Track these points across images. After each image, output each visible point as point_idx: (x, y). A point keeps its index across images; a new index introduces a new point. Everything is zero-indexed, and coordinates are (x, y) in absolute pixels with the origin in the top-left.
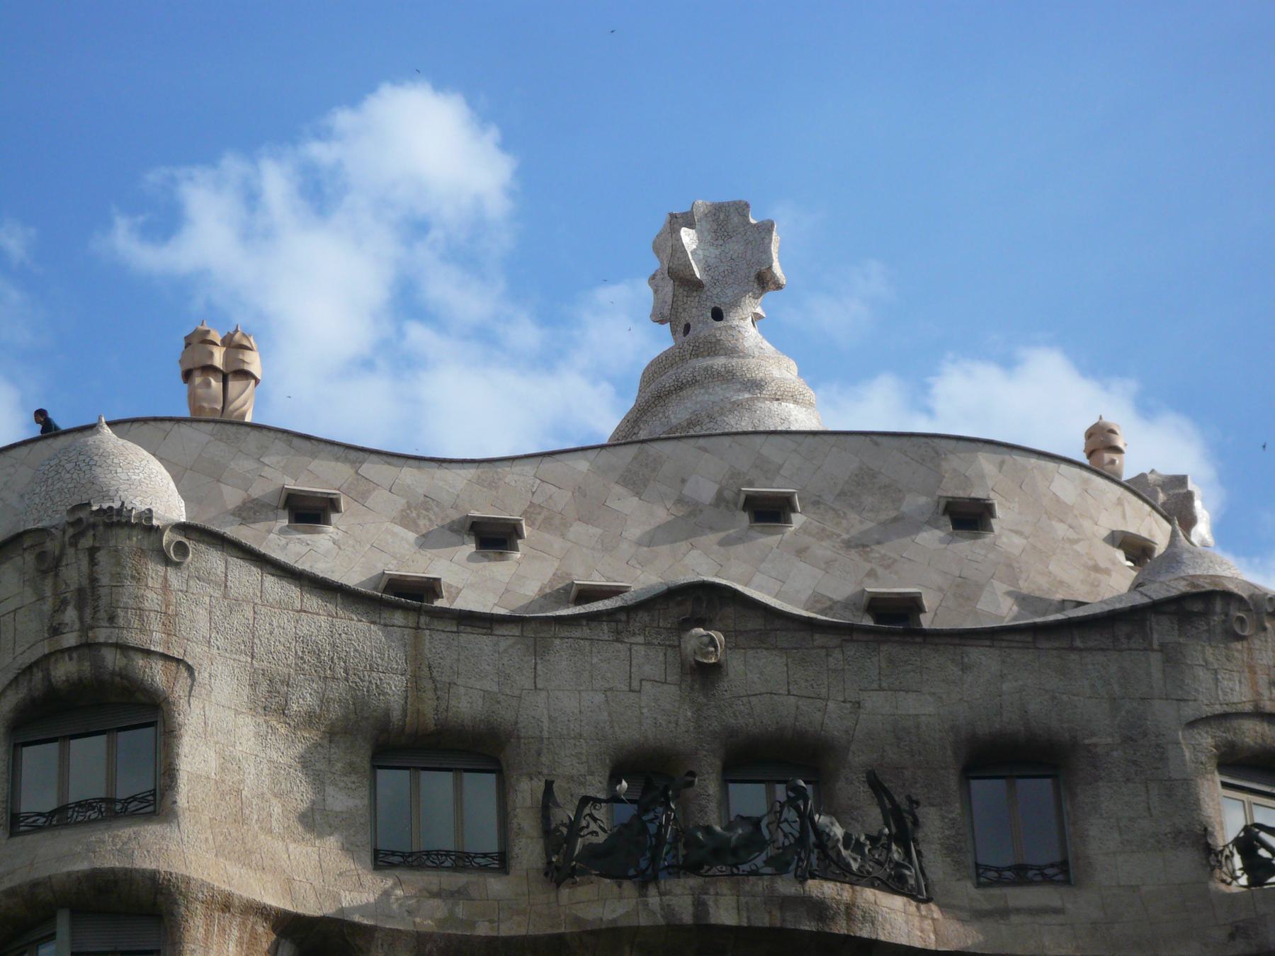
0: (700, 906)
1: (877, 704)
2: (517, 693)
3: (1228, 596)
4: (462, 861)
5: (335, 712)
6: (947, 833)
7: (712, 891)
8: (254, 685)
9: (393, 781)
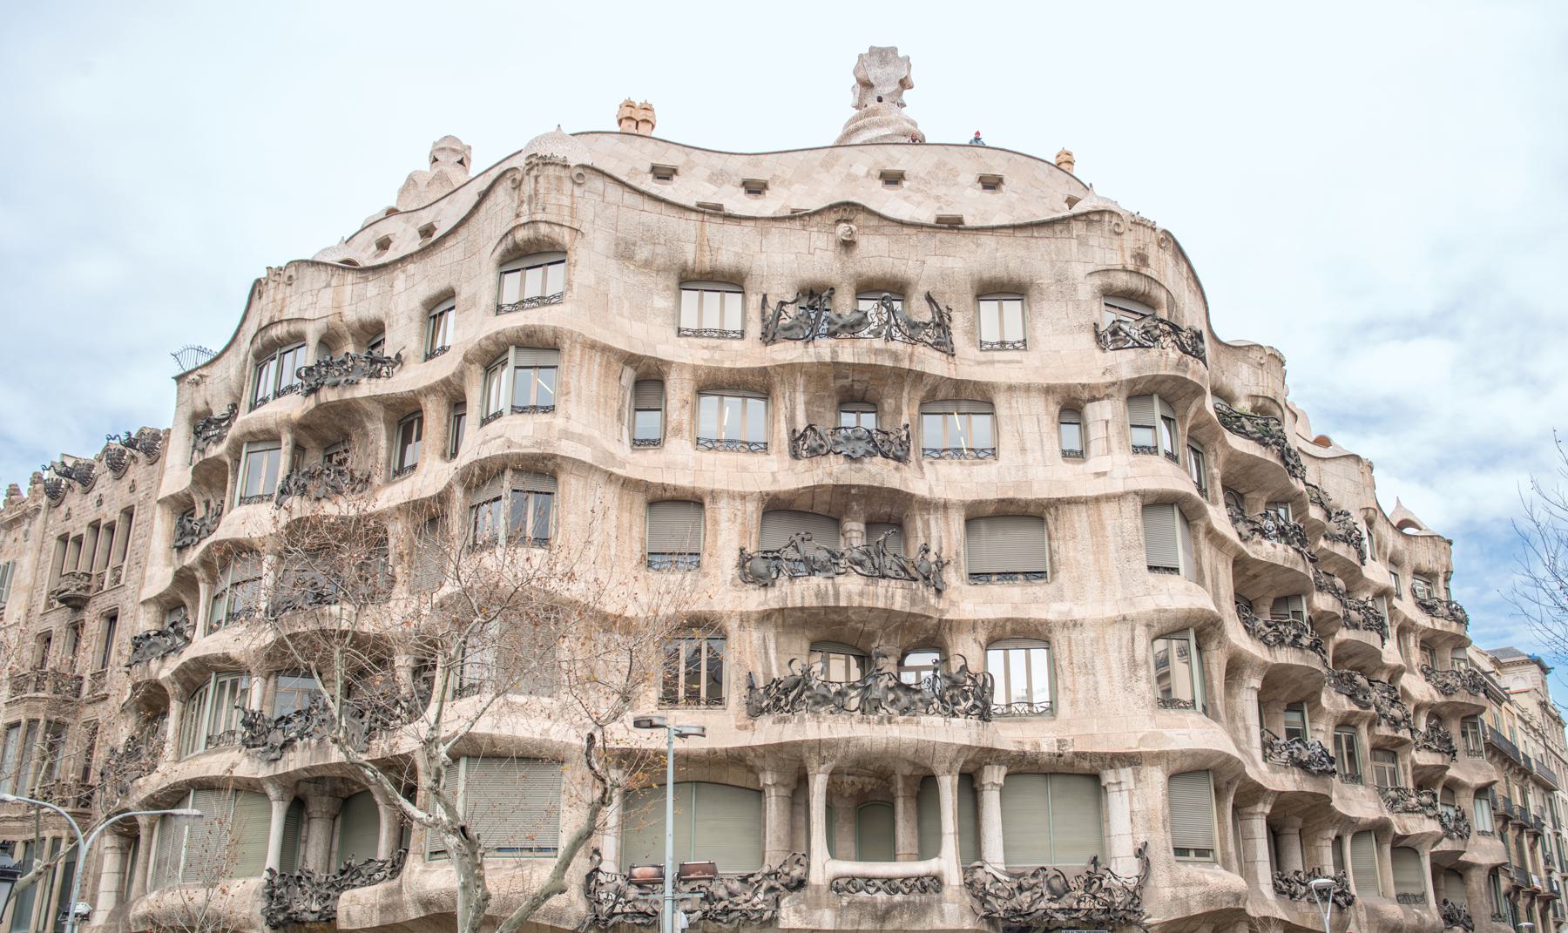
0: (834, 352)
3: (1111, 212)
4: (723, 334)
5: (660, 261)
8: (617, 245)
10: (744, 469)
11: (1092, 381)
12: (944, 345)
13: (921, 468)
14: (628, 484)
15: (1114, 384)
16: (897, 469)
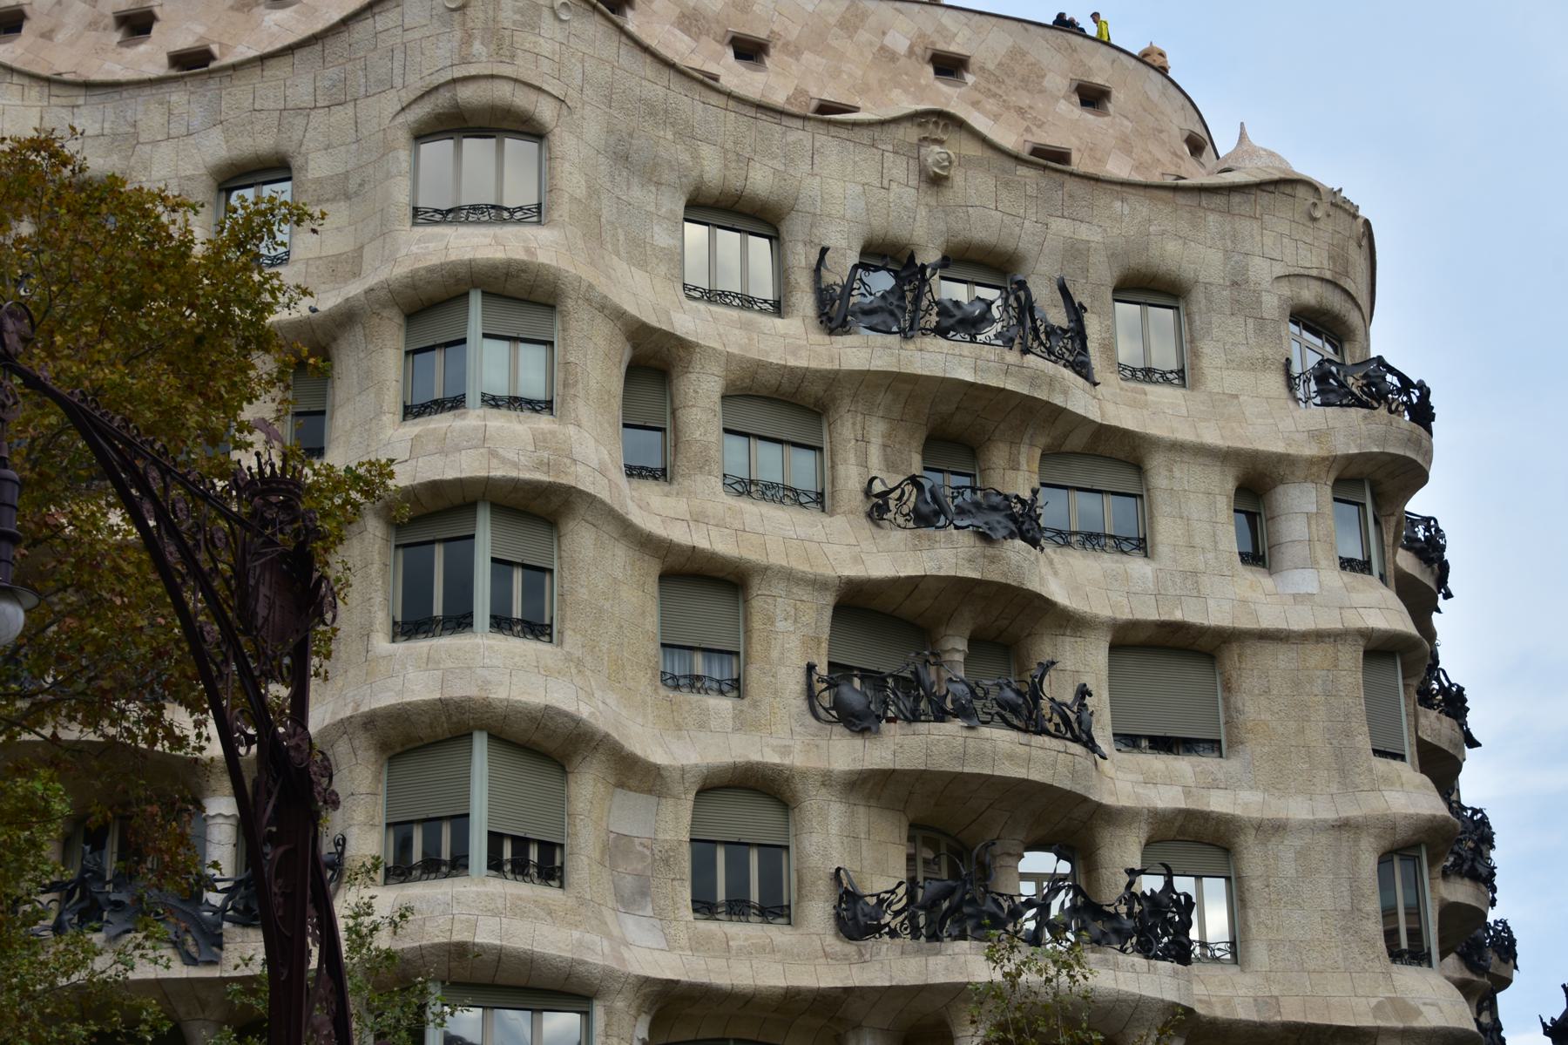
1: (1061, 227)
4: (747, 302)
9: (696, 234)
11: (1292, 451)
12: (1082, 368)
14: (646, 543)
15: (1324, 459)
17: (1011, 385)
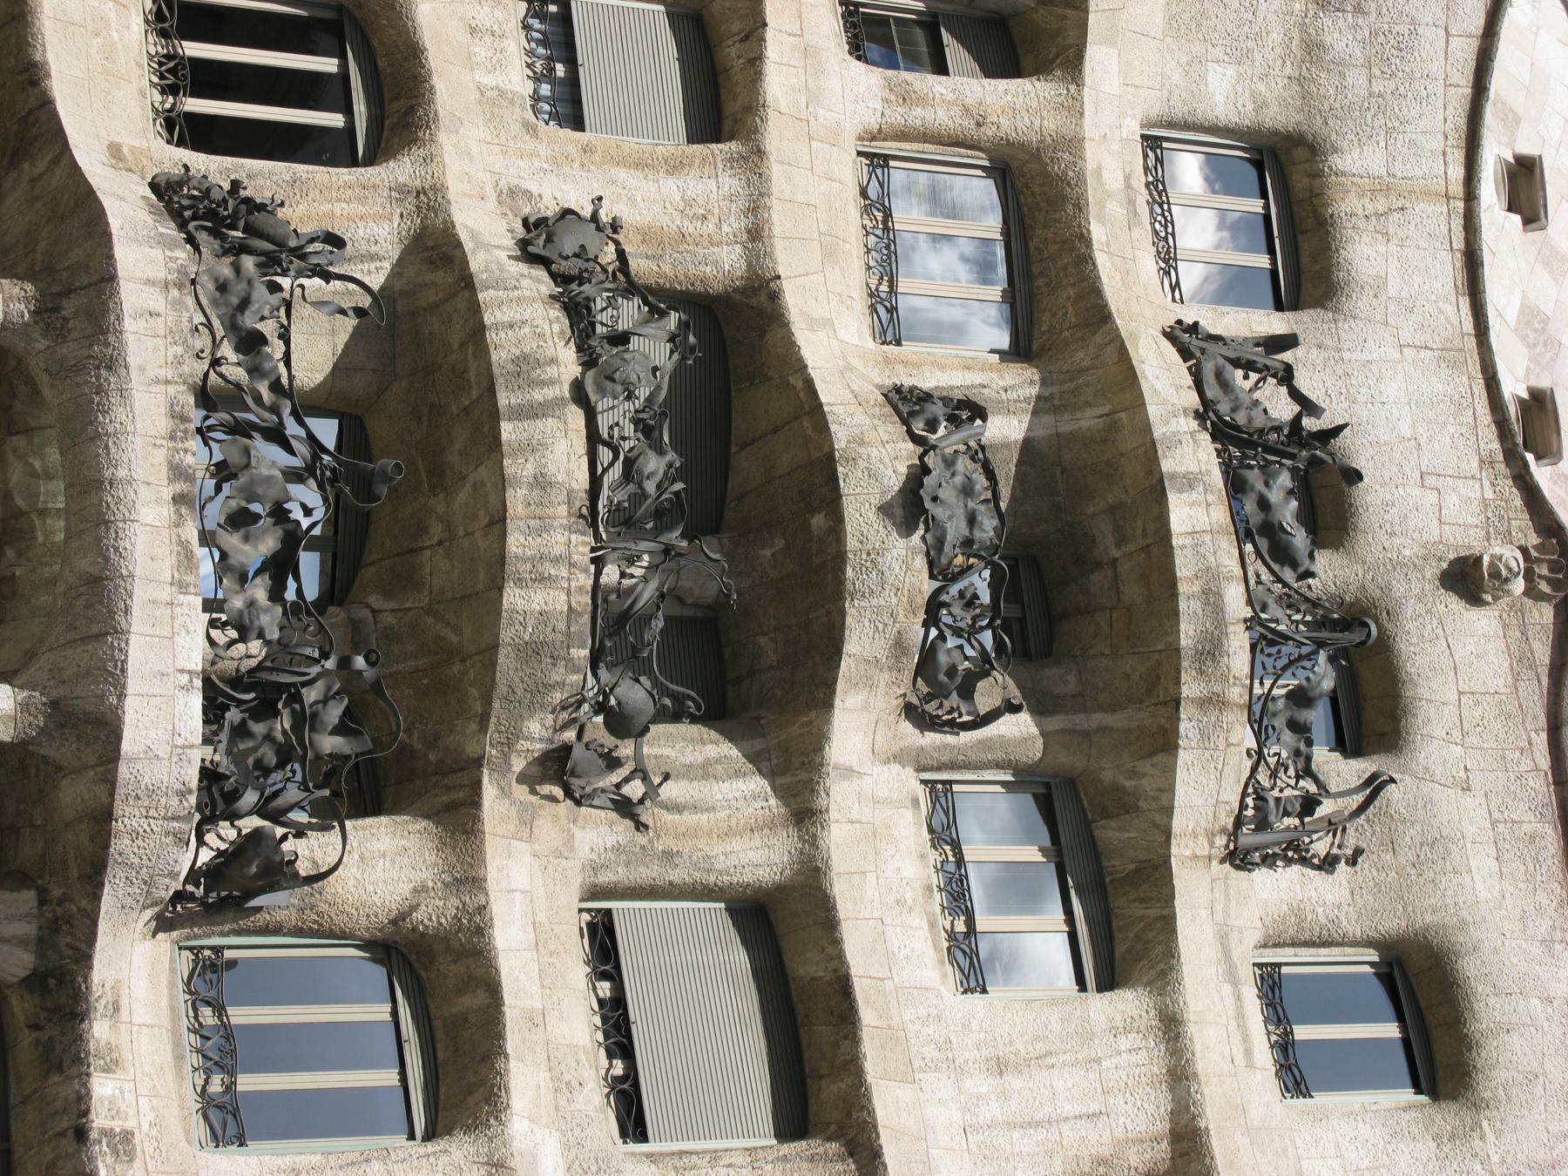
0: (1190, 482)
2: (1391, 321)
5: (1327, 84)
6: (1320, 910)
7: (1210, 498)
10: (830, 254)
13: (898, 758)
16: (899, 646)
17: (1189, 606)
